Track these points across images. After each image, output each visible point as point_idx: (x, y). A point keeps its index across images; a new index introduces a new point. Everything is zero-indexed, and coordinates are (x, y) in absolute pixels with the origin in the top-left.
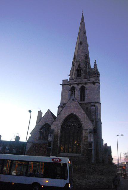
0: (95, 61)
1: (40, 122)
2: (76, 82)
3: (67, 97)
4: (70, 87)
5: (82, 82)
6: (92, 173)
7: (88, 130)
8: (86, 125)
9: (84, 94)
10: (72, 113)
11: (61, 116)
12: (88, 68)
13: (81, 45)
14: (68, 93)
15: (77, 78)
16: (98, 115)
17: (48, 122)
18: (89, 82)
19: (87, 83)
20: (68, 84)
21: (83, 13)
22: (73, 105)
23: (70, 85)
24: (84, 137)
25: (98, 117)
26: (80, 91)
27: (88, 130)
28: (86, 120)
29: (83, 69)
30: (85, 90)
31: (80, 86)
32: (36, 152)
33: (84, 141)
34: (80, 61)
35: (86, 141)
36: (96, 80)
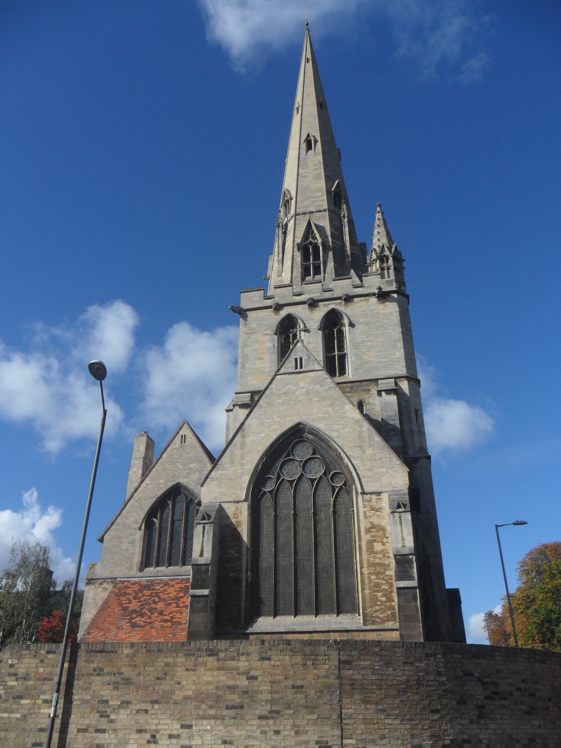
1: (147, 481)
4: (275, 318)
5: (328, 295)
6: (481, 708)
7: (385, 497)
8: (368, 473)
9: (341, 347)
10: (299, 424)
11: (248, 440)
15: (303, 279)
16: (412, 431)
17: (183, 481)
22: (302, 384)
23: (278, 308)
24: (368, 531)
25: (416, 438)
27: (385, 497)
28: (369, 451)
30: (346, 329)
32: (134, 625)
33: (371, 550)
34: (311, 213)
35: (378, 547)
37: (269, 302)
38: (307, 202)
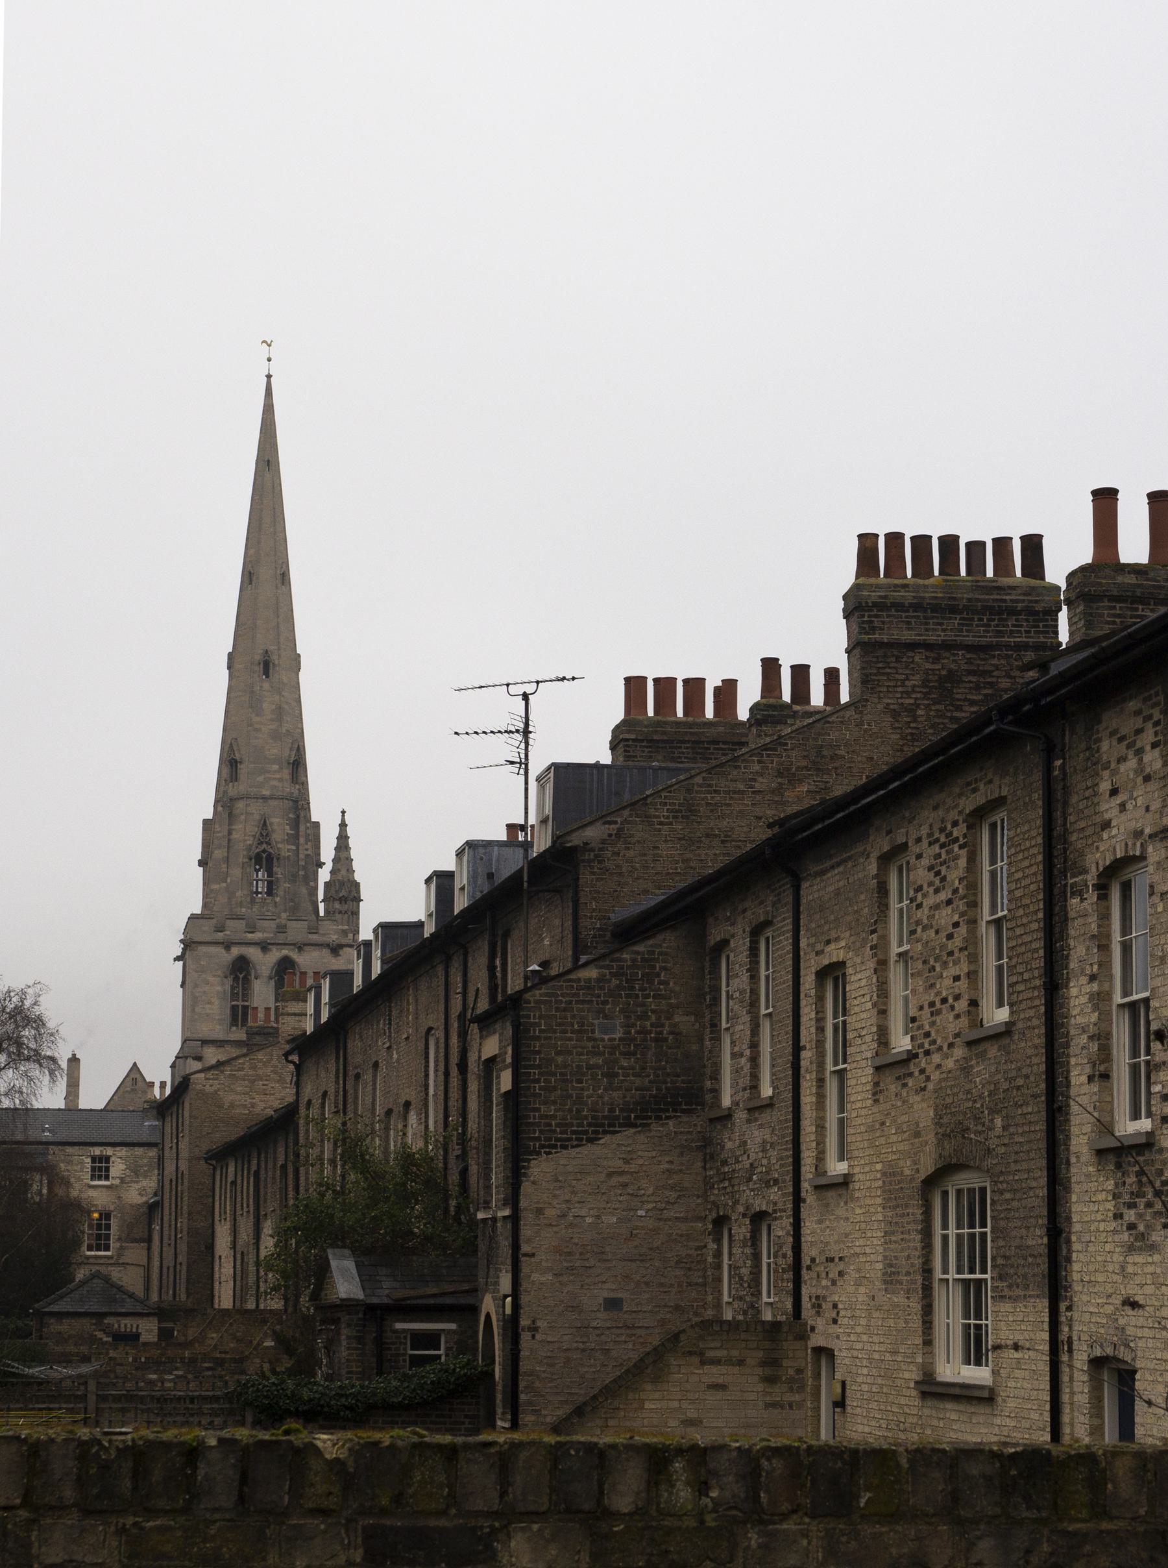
0: (343, 812)
2: (258, 936)
3: (216, 1007)
4: (227, 957)
5: (281, 938)
12: (302, 840)
13: (266, 673)
14: (219, 988)
18: (314, 938)
19: (305, 945)
20: (216, 943)
21: (269, 377)
26: (272, 983)
29: (283, 854)
31: (275, 955)
36: (345, 933)
37: (220, 936)
38: (261, 779)
